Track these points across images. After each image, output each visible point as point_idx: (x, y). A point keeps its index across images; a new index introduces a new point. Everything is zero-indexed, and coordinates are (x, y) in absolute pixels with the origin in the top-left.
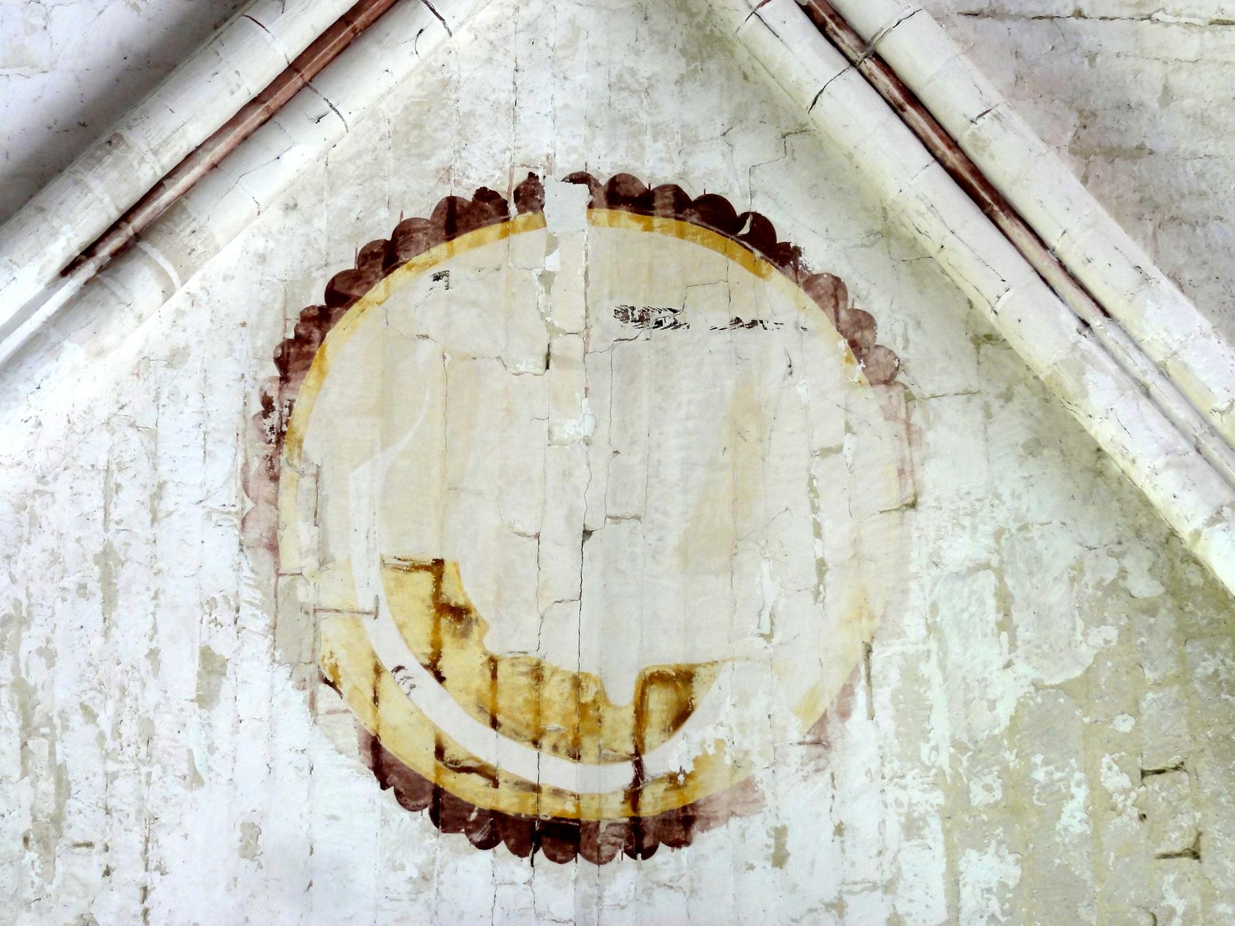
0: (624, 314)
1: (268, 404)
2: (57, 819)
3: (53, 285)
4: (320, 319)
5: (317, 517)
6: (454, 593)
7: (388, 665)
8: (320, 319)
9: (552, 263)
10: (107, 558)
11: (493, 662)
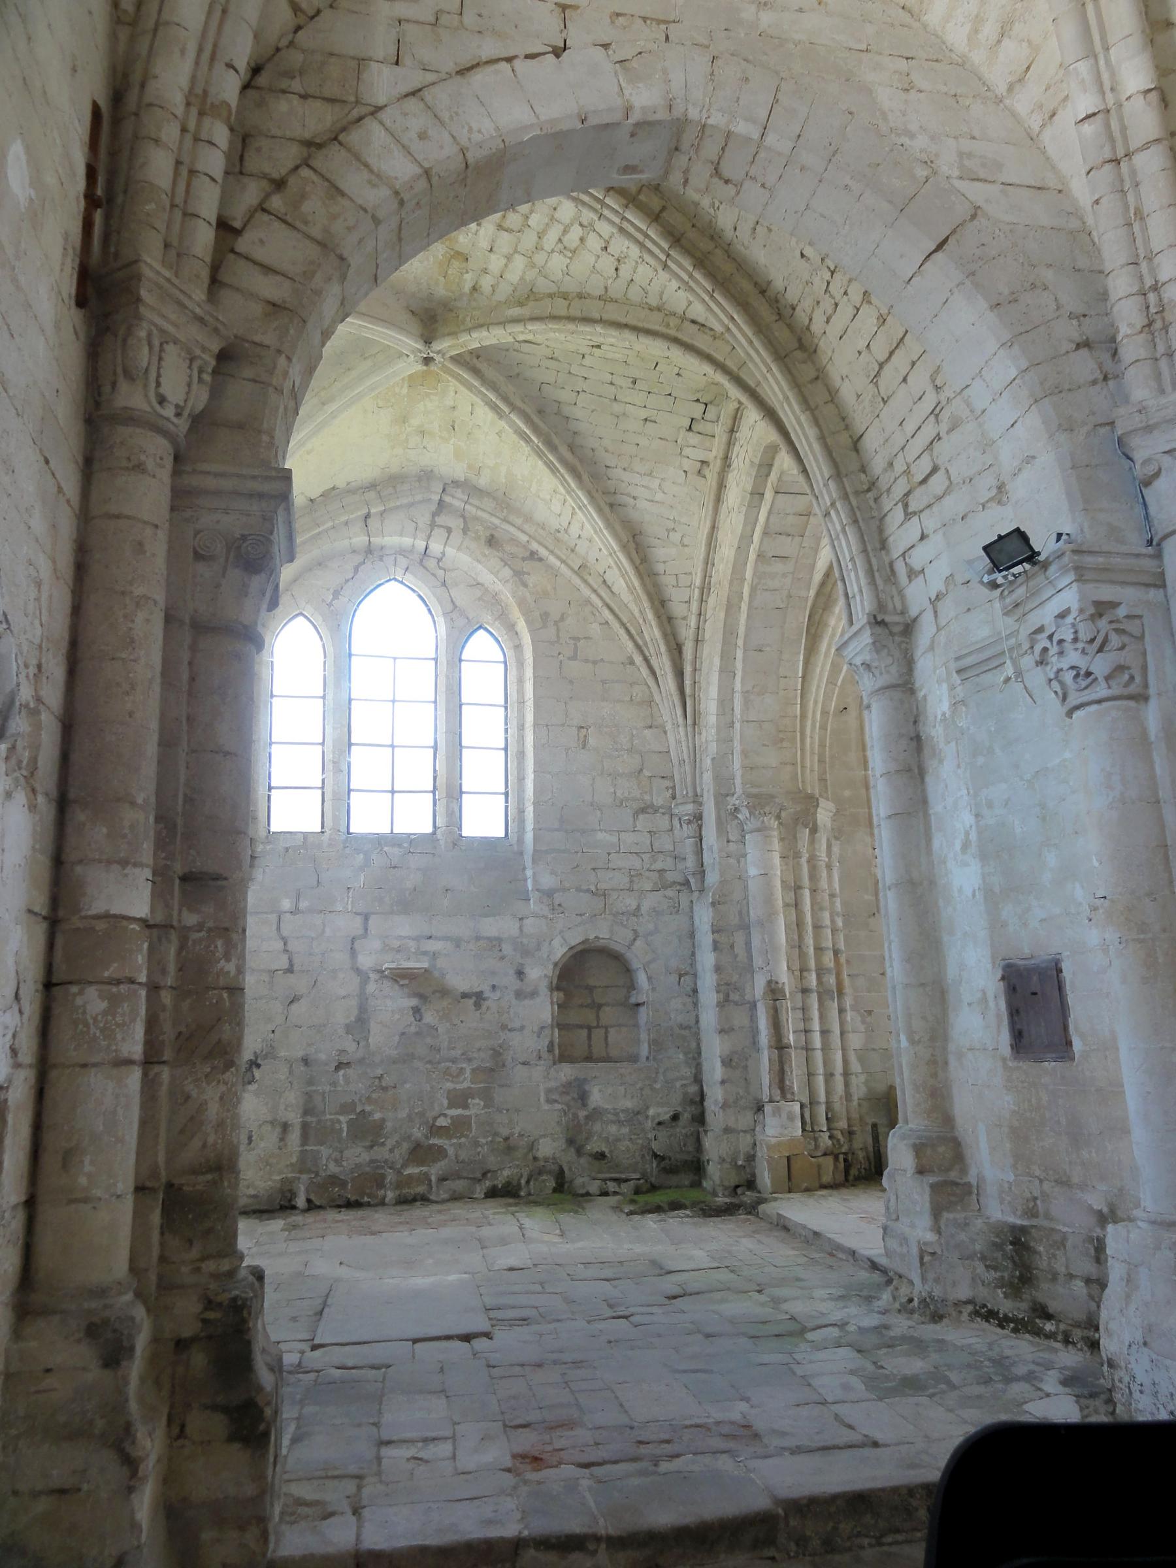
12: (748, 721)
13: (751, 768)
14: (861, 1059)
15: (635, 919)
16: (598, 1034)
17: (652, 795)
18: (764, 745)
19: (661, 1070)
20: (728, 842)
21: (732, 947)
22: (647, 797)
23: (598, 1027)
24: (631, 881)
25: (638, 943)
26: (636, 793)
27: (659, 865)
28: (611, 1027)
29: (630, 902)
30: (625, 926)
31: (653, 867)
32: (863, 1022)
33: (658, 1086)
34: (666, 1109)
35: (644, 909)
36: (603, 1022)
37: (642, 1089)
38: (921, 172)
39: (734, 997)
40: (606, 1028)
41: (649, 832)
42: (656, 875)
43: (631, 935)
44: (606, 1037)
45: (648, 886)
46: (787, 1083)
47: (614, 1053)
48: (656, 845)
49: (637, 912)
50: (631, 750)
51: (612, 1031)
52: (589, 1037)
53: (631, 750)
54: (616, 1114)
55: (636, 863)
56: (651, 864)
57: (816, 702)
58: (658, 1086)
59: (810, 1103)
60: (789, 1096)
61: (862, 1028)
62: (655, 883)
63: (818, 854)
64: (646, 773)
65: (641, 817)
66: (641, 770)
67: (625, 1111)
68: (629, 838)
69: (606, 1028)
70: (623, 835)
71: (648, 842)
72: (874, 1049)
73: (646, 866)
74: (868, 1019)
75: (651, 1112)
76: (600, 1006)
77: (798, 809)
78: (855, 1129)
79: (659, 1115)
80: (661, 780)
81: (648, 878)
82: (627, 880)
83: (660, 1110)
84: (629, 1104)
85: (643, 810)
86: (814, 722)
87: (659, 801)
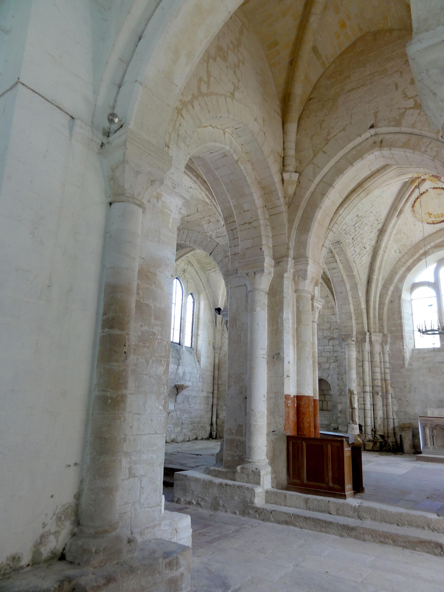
0: (437, 194)
1: (412, 210)
2: (408, 237)
3: (396, 218)
4: (414, 204)
5: (418, 214)
6: (430, 213)
7: (426, 218)
8: (414, 204)
9: (430, 194)
10: (405, 223)
11: (434, 216)
12: (343, 313)
13: (344, 327)
14: (396, 414)
15: (328, 370)
16: (325, 403)
17: (333, 334)
18: (348, 320)
19: (335, 414)
20: (342, 348)
21: (342, 379)
22: (332, 335)
23: (325, 401)
24: (327, 360)
25: (329, 377)
26: (329, 334)
27: (335, 355)
28: (328, 401)
29: (327, 366)
30: (326, 373)
31: (334, 356)
32: (398, 402)
33: (334, 418)
34: (336, 425)
35: (331, 368)
36: (326, 399)
37: (329, 419)
38: (209, 240)
39: (343, 393)
40: (327, 401)
41: (333, 345)
42: (334, 358)
43: (327, 375)
44: (327, 404)
45: (332, 361)
46: (354, 419)
47: (329, 408)
48: (335, 349)
49: (329, 369)
50: (328, 322)
51: (329, 402)
52: (322, 404)
53: (328, 322)
54: (322, 425)
55: (329, 354)
56: (333, 355)
57: (375, 302)
58: (334, 418)
59: (365, 426)
60: (355, 423)
61: (397, 404)
62: (334, 360)
63: (374, 350)
64: (332, 328)
65: (330, 341)
66: (330, 328)
67: (325, 424)
68: (327, 348)
69: (327, 401)
70: (325, 347)
71: (332, 348)
72: (401, 411)
73: (332, 355)
74: (399, 401)
75: (332, 425)
76: (325, 395)
77: (363, 337)
78: (389, 435)
79: (334, 426)
80: (336, 330)
81: (332, 359)
82: (326, 359)
83: (335, 425)
84: (326, 422)
85: (331, 339)
86: (374, 308)
87: (335, 336)
